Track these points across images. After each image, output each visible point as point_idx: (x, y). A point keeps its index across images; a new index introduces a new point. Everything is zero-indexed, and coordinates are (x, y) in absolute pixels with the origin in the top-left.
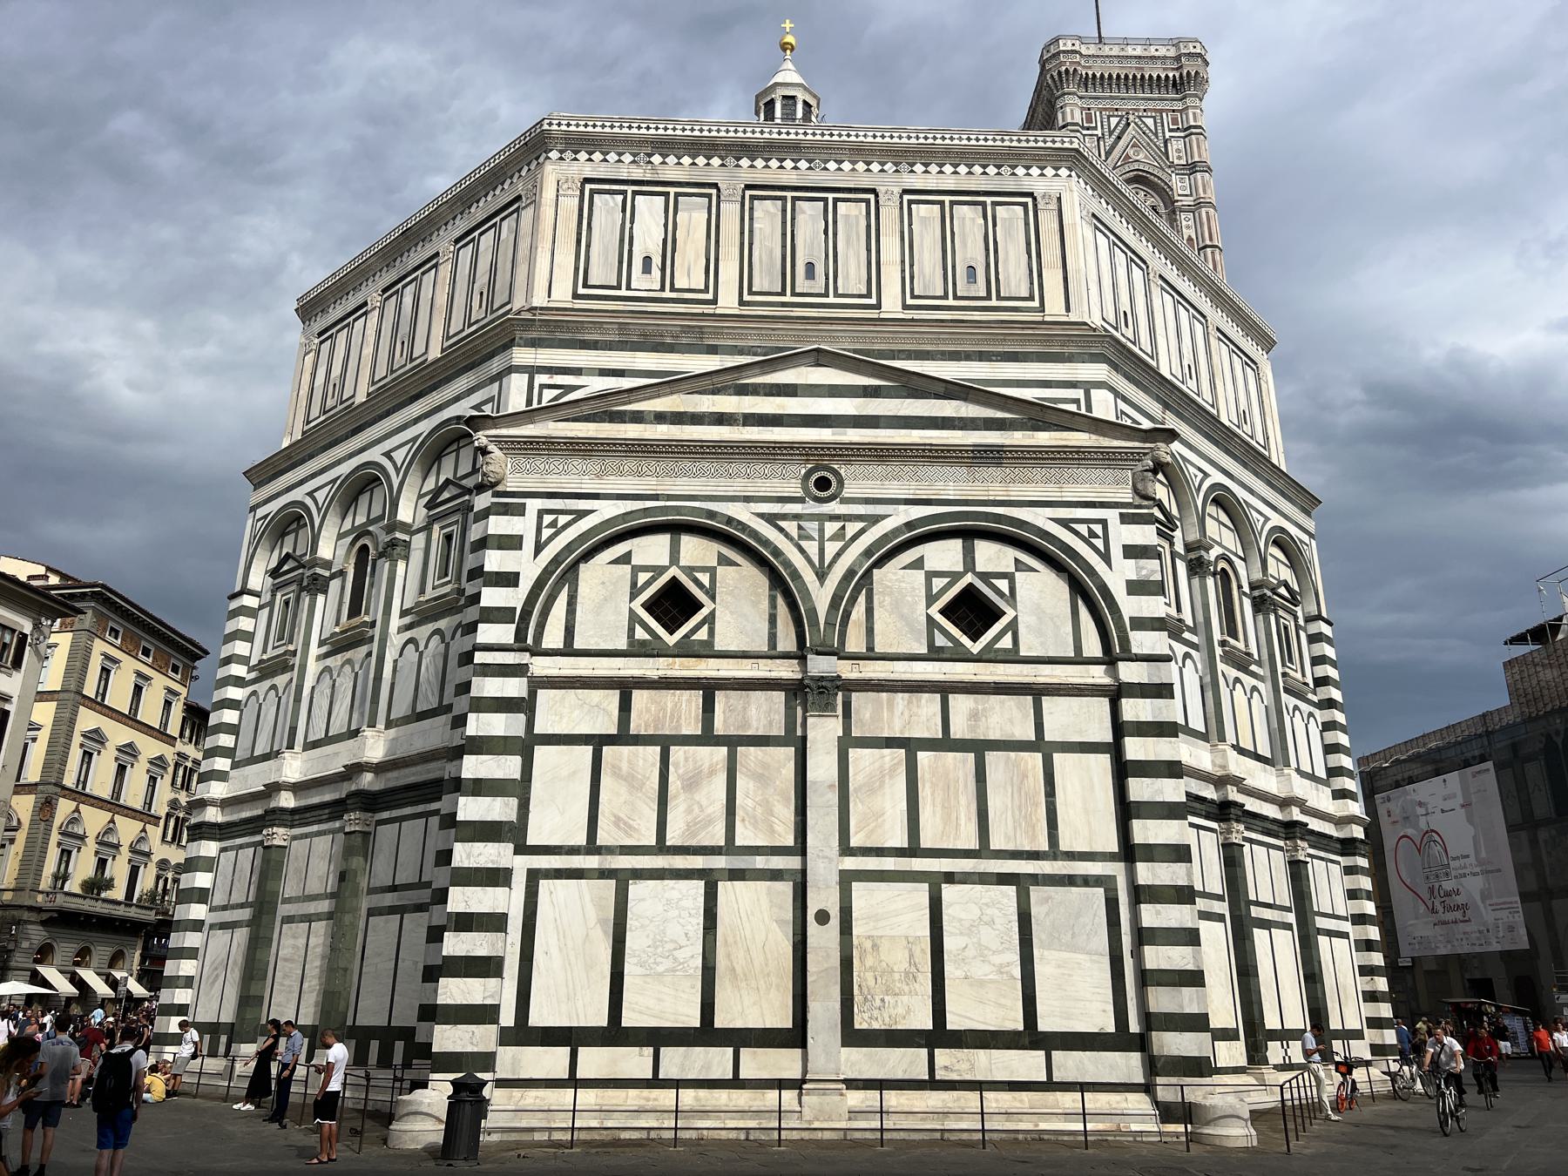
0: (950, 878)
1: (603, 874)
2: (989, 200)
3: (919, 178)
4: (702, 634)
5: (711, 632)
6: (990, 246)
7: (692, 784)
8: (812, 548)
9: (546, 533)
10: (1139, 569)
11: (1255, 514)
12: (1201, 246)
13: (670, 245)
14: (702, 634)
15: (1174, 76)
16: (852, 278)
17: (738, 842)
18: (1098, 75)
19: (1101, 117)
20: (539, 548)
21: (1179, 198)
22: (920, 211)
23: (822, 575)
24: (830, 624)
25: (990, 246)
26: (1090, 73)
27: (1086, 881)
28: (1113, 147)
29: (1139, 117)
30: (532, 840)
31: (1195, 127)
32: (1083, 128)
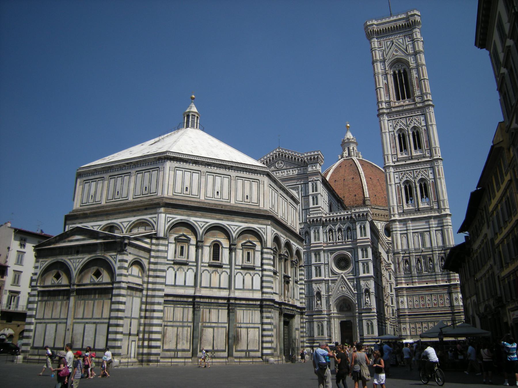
0: (87, 323)
4: (60, 282)
5: (62, 281)
6: (150, 182)
7: (56, 308)
8: (74, 264)
9: (42, 265)
10: (120, 264)
11: (232, 227)
12: (420, 80)
13: (96, 192)
14: (60, 282)
15: (407, 23)
16: (124, 195)
19: (384, 43)
20: (41, 267)
21: (412, 65)
22: (139, 175)
23: (75, 269)
24: (75, 279)
25: (150, 182)
28: (388, 52)
30: (37, 317)
31: (416, 39)
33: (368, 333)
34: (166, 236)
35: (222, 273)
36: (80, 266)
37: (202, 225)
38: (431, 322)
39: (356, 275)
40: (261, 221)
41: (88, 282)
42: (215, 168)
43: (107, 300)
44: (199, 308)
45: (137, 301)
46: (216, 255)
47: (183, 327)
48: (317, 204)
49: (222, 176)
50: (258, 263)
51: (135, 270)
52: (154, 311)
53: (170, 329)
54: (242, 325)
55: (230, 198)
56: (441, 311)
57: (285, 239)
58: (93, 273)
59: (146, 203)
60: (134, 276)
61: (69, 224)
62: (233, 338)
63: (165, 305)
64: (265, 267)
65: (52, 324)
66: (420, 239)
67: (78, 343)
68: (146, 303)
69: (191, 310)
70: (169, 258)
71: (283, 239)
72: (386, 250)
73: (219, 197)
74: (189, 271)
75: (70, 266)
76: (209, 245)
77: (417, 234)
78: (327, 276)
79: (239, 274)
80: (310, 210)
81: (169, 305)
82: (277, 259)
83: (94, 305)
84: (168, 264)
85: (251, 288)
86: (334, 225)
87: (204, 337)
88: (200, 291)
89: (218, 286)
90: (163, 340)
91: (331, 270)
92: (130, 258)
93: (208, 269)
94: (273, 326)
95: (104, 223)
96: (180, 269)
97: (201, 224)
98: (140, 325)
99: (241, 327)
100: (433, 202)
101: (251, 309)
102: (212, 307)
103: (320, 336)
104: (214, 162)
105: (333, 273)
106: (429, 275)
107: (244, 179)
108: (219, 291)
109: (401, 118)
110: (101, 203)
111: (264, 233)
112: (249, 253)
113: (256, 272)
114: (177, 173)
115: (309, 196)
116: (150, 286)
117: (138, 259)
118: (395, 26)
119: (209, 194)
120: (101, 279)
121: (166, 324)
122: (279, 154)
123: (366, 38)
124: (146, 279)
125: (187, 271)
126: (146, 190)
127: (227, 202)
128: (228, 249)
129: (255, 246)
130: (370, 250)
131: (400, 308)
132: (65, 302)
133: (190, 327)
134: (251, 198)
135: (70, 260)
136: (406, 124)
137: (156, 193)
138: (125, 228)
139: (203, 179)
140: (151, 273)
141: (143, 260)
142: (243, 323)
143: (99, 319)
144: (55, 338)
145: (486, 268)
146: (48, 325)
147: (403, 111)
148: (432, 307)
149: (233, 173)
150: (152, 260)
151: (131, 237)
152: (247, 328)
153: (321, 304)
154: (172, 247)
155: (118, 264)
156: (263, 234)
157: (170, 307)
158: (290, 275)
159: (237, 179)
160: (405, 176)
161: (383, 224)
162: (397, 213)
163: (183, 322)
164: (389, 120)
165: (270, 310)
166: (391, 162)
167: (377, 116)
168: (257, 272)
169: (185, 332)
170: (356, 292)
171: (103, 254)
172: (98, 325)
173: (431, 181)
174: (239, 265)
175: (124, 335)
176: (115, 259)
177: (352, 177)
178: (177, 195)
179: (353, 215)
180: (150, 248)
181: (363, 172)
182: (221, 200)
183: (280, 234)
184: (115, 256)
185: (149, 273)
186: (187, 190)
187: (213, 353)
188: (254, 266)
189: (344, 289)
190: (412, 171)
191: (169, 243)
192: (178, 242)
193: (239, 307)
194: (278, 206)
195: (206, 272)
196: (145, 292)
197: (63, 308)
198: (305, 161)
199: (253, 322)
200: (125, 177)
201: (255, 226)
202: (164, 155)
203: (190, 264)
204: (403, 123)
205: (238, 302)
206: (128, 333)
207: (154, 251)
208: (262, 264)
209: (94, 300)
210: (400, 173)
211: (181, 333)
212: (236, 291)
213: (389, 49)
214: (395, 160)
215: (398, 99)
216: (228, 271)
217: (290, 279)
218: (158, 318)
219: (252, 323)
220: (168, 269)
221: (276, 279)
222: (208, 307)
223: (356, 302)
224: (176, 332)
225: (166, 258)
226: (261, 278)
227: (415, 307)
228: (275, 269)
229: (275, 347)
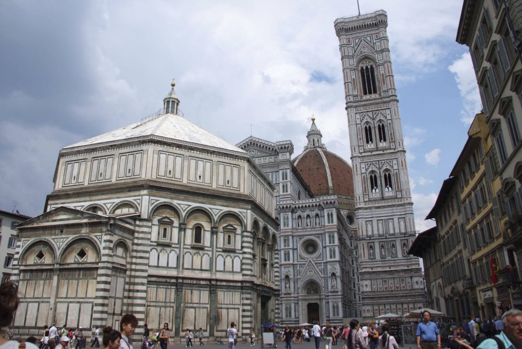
0: (71, 302)
1: (26, 302)
2: (135, 153)
3: (123, 150)
8: (58, 244)
9: (24, 244)
11: (214, 210)
14: (43, 261)
17: (44, 296)
18: (351, 27)
20: (23, 247)
22: (122, 157)
23: (59, 249)
24: (59, 258)
26: (348, 27)
27: (90, 302)
29: (365, 38)
31: (383, 37)
32: (347, 45)
33: (334, 315)
34: (150, 218)
35: (203, 255)
36: (64, 246)
37: (185, 208)
38: (393, 304)
39: (323, 260)
40: (242, 205)
41: (73, 262)
42: (198, 152)
43: (92, 280)
44: (182, 288)
45: (121, 281)
46: (198, 238)
47: (166, 307)
48: (287, 191)
49: (205, 160)
50: (238, 247)
51: (120, 251)
52: (138, 291)
53: (152, 309)
54: (223, 306)
55: (211, 183)
56: (403, 294)
57: (263, 224)
58: (77, 253)
59: (130, 185)
60: (118, 256)
61: (51, 205)
62: (214, 319)
63: (148, 286)
64: (245, 250)
65: (34, 303)
66: (384, 226)
67: (61, 322)
68: (130, 283)
69: (173, 291)
70: (153, 240)
71: (261, 223)
72: (350, 237)
73: (201, 181)
74: (172, 252)
75: (53, 245)
76: (191, 227)
77: (381, 221)
78: (296, 260)
79: (220, 257)
80: (281, 197)
81: (152, 286)
82: (256, 242)
83: (78, 285)
84: (151, 245)
85: (231, 270)
86: (303, 212)
87: (186, 317)
88: (182, 272)
89: (199, 268)
90: (146, 319)
91: (299, 255)
92: (115, 238)
93: (190, 251)
94: (252, 307)
95: (87, 204)
96: (163, 251)
97: (184, 207)
98: (123, 304)
99: (221, 308)
100: (396, 191)
101: (231, 290)
102: (194, 288)
103: (288, 318)
104: (196, 147)
105: (302, 258)
106: (391, 260)
107: (225, 164)
108: (201, 273)
109: (367, 112)
110: (84, 184)
111: (245, 217)
112: (229, 236)
113: (236, 255)
114: (161, 156)
115: (279, 184)
116: (134, 267)
117: (123, 239)
118: (364, 25)
119: (192, 178)
120: (86, 259)
121: (149, 304)
122: (251, 143)
123: (336, 35)
124: (129, 260)
125: (170, 252)
126: (129, 172)
127: (209, 186)
128: (210, 232)
129: (235, 229)
130: (336, 235)
131: (365, 291)
132: (48, 281)
133: (173, 307)
134: (232, 183)
135: (53, 239)
136: (372, 117)
137: (139, 175)
138: (108, 209)
139: (186, 163)
140: (134, 254)
141: (128, 241)
142: (224, 304)
143: (83, 298)
144: (37, 317)
145: (454, 252)
146: (30, 304)
147: (369, 105)
148: (395, 290)
149: (215, 158)
150: (136, 241)
151: (117, 217)
152: (228, 309)
153: (289, 287)
154: (155, 229)
155: (103, 245)
156: (244, 218)
157: (153, 287)
158: (266, 258)
159: (219, 164)
160: (371, 166)
161: (345, 212)
162: (363, 201)
163: (165, 302)
164: (357, 113)
165: (249, 291)
166: (358, 153)
167: (345, 109)
168: (238, 255)
169: (168, 312)
170: (323, 276)
171: (88, 234)
172: (82, 304)
173: (395, 171)
174: (220, 248)
175: (109, 314)
176: (100, 240)
177: (317, 167)
178: (161, 178)
179: (321, 203)
180: (133, 229)
181: (327, 163)
182: (203, 184)
183: (259, 218)
184: (100, 237)
185: (132, 254)
186: (170, 173)
187: (194, 333)
188: (234, 249)
189: (311, 273)
190: (377, 162)
191: (152, 225)
192: (161, 224)
193: (220, 288)
194: (256, 191)
195: (188, 254)
196: (128, 273)
197: (46, 287)
198: (276, 150)
199: (233, 303)
200: (108, 159)
201: (236, 210)
202: (148, 138)
203: (173, 246)
204: (369, 117)
205: (219, 283)
206: (112, 312)
207: (138, 232)
208: (242, 247)
209: (78, 279)
210: (366, 163)
211: (163, 314)
212: (217, 273)
213: (357, 46)
214: (362, 151)
215: (365, 93)
216: (210, 253)
217: (267, 262)
218: (141, 298)
219: (232, 304)
220: (151, 250)
221: (254, 262)
222: (190, 288)
223: (323, 285)
224: (159, 312)
225: (149, 239)
226: (241, 261)
227: (379, 290)
228: (254, 252)
229: (253, 327)
